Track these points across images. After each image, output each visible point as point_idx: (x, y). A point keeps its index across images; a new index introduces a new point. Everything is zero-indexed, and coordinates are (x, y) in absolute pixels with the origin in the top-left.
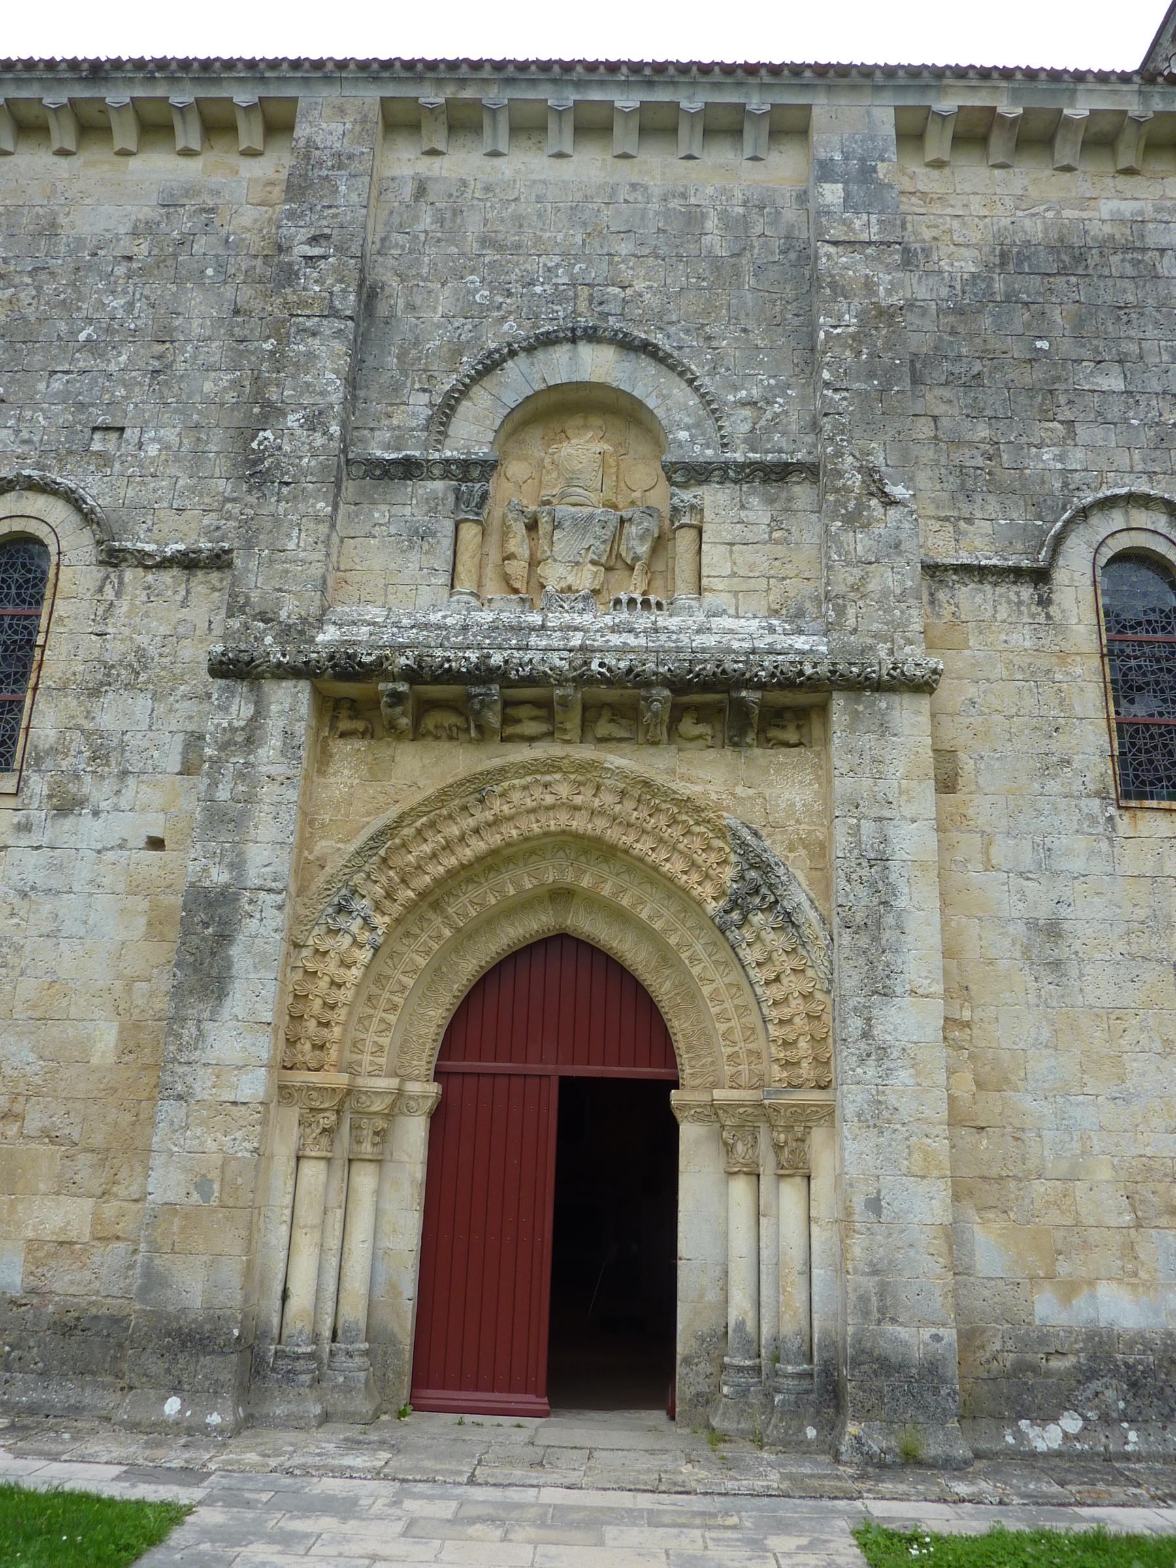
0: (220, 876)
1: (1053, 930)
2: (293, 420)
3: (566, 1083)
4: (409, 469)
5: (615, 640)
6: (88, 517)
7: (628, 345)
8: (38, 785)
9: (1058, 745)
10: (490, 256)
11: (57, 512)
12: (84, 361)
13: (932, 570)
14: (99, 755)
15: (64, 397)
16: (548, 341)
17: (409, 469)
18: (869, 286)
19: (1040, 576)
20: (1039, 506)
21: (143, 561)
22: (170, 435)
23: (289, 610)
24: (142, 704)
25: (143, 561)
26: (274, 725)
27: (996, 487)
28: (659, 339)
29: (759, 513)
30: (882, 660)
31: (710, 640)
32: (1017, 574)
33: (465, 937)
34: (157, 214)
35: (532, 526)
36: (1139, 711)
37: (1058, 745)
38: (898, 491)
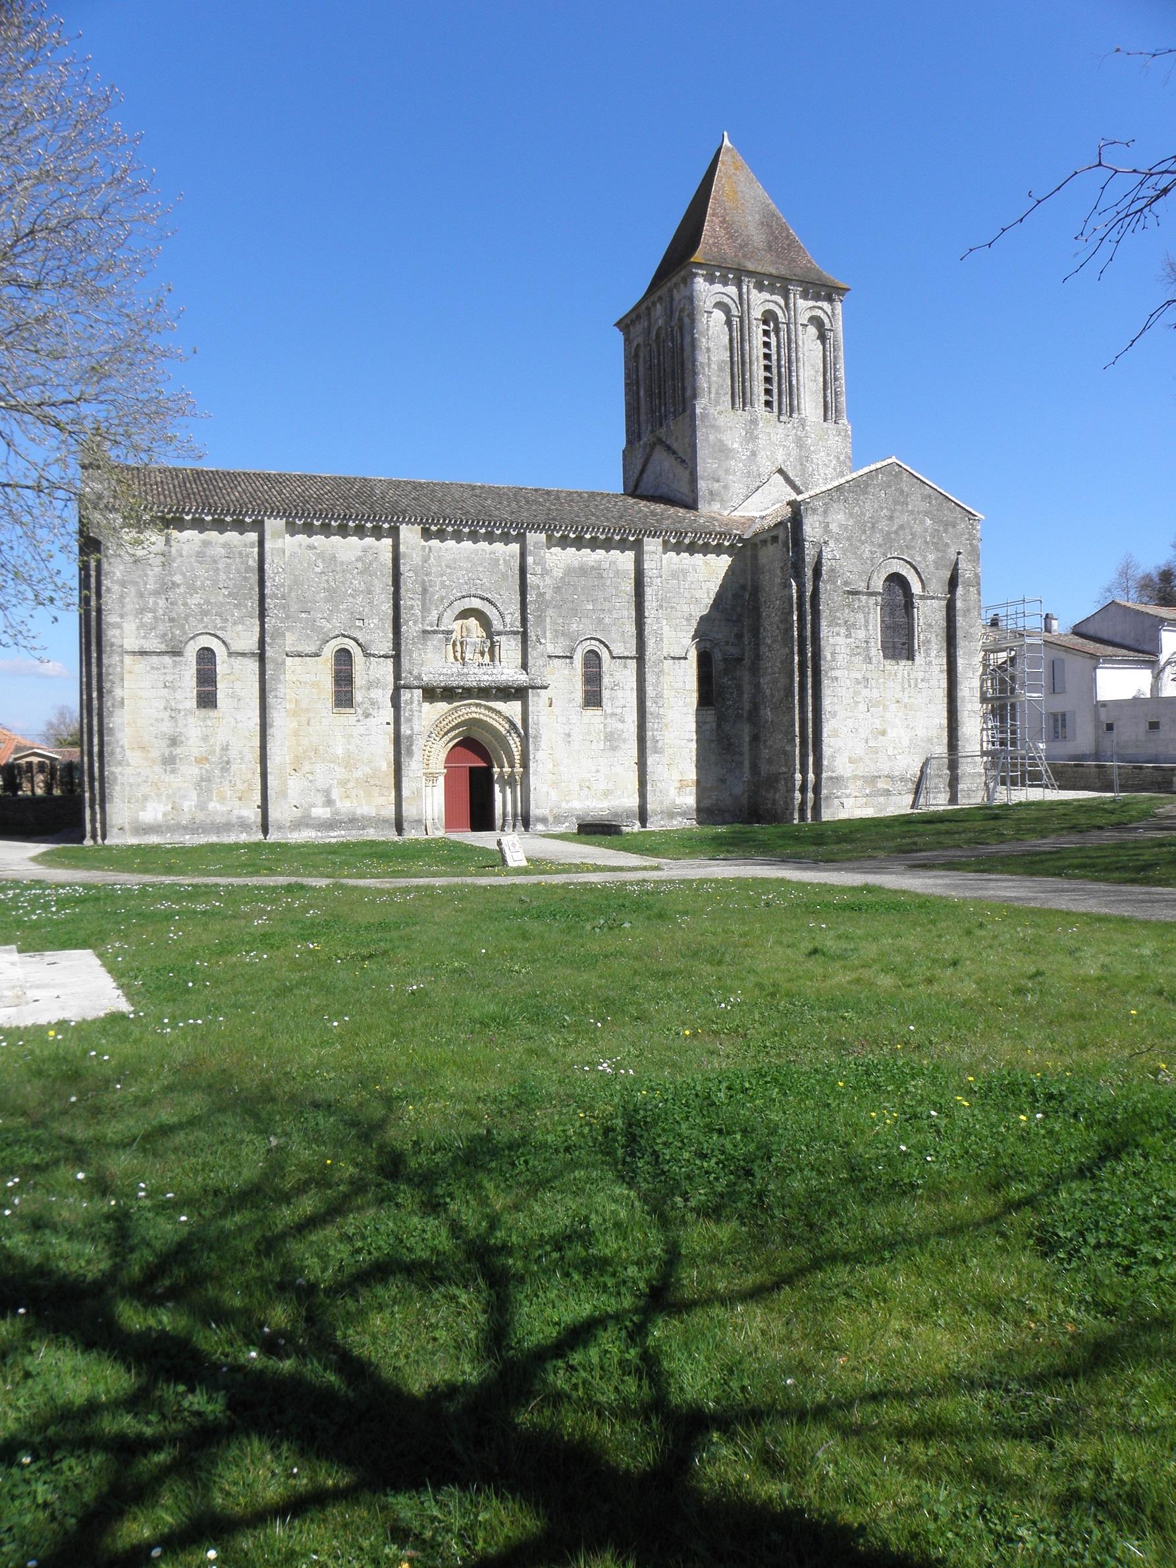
0: (409, 732)
1: (569, 735)
2: (411, 623)
3: (471, 768)
4: (435, 632)
5: (486, 677)
6: (360, 645)
7: (482, 599)
8: (360, 711)
9: (572, 696)
10: (449, 571)
11: (352, 643)
12: (351, 600)
13: (549, 657)
14: (373, 704)
15: (347, 610)
16: (464, 597)
17: (435, 632)
18: (538, 587)
19: (571, 658)
20: (573, 640)
21: (374, 656)
22: (376, 621)
23: (415, 673)
24: (380, 691)
25: (374, 656)
26: (415, 698)
27: (563, 634)
28: (489, 596)
29: (513, 643)
30: (539, 682)
31: (504, 677)
32: (567, 657)
33: (451, 740)
34: (361, 554)
35: (462, 643)
36: (589, 688)
37: (572, 696)
38: (543, 641)
